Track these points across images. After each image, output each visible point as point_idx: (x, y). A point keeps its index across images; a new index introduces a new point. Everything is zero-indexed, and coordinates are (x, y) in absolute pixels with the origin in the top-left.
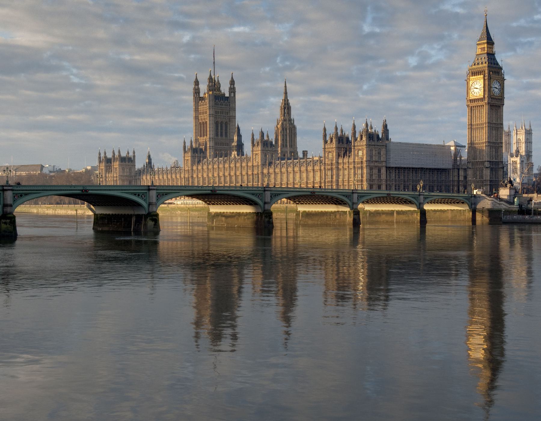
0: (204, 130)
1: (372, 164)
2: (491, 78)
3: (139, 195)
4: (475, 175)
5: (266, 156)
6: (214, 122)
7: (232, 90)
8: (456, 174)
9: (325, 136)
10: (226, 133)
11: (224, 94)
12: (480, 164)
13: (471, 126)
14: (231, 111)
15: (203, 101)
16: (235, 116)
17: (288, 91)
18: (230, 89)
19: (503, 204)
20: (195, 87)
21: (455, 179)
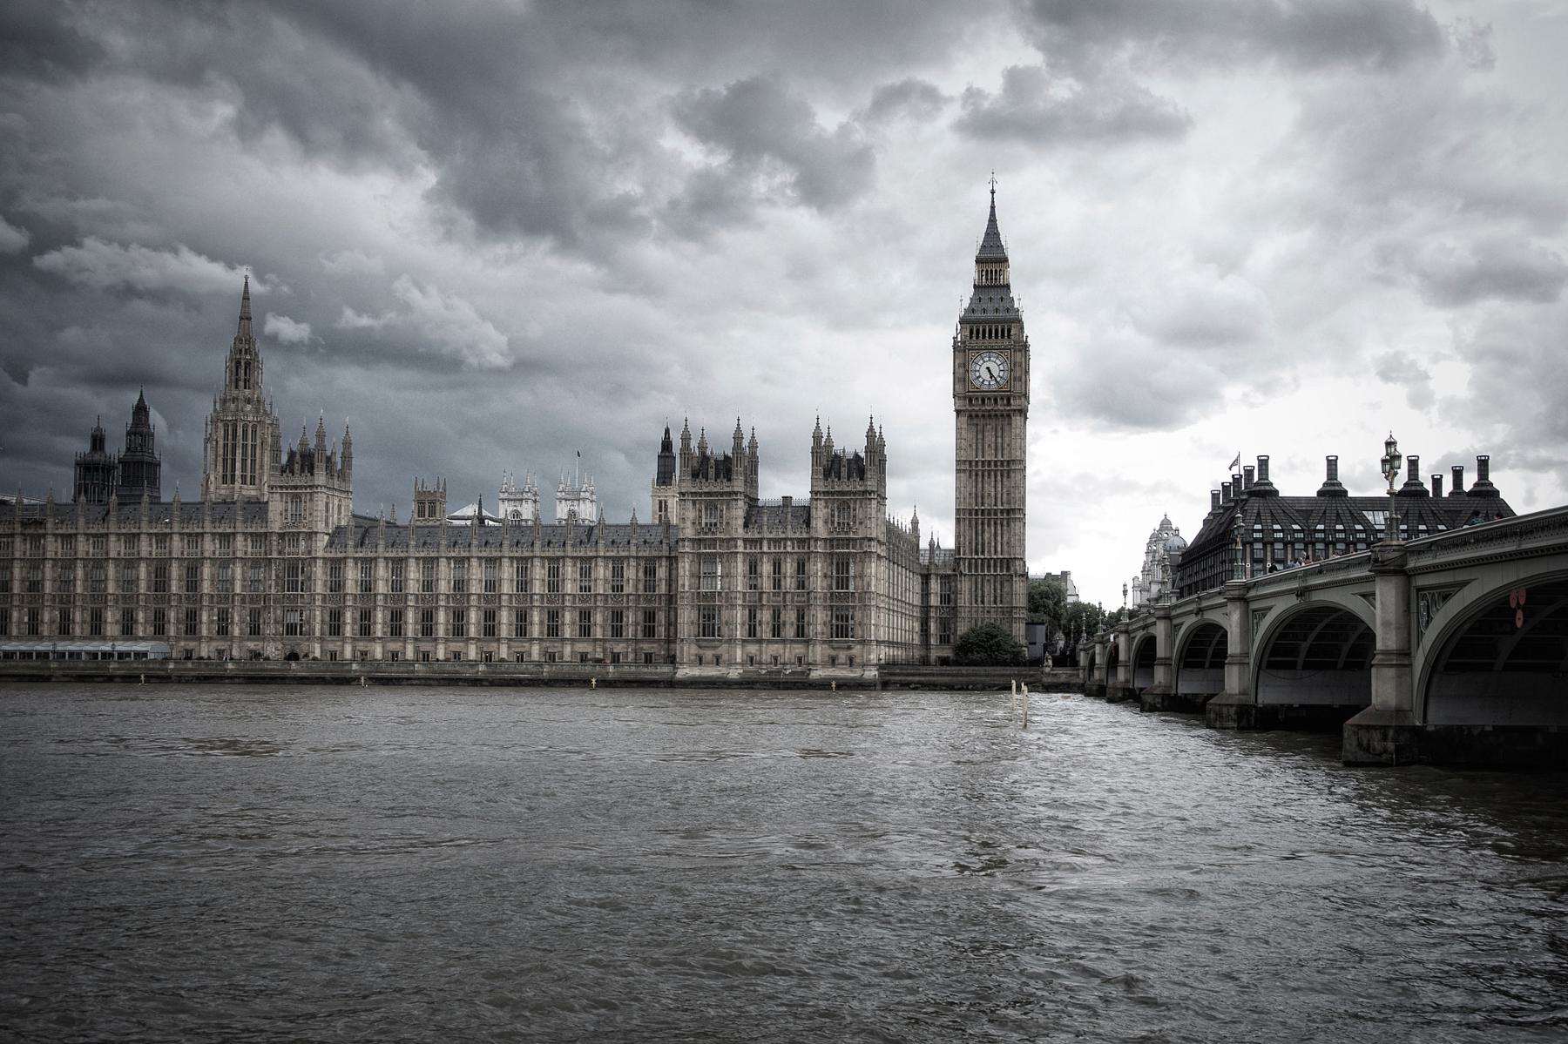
2: (1026, 351)
4: (980, 592)
8: (918, 588)
12: (995, 566)
21: (915, 603)
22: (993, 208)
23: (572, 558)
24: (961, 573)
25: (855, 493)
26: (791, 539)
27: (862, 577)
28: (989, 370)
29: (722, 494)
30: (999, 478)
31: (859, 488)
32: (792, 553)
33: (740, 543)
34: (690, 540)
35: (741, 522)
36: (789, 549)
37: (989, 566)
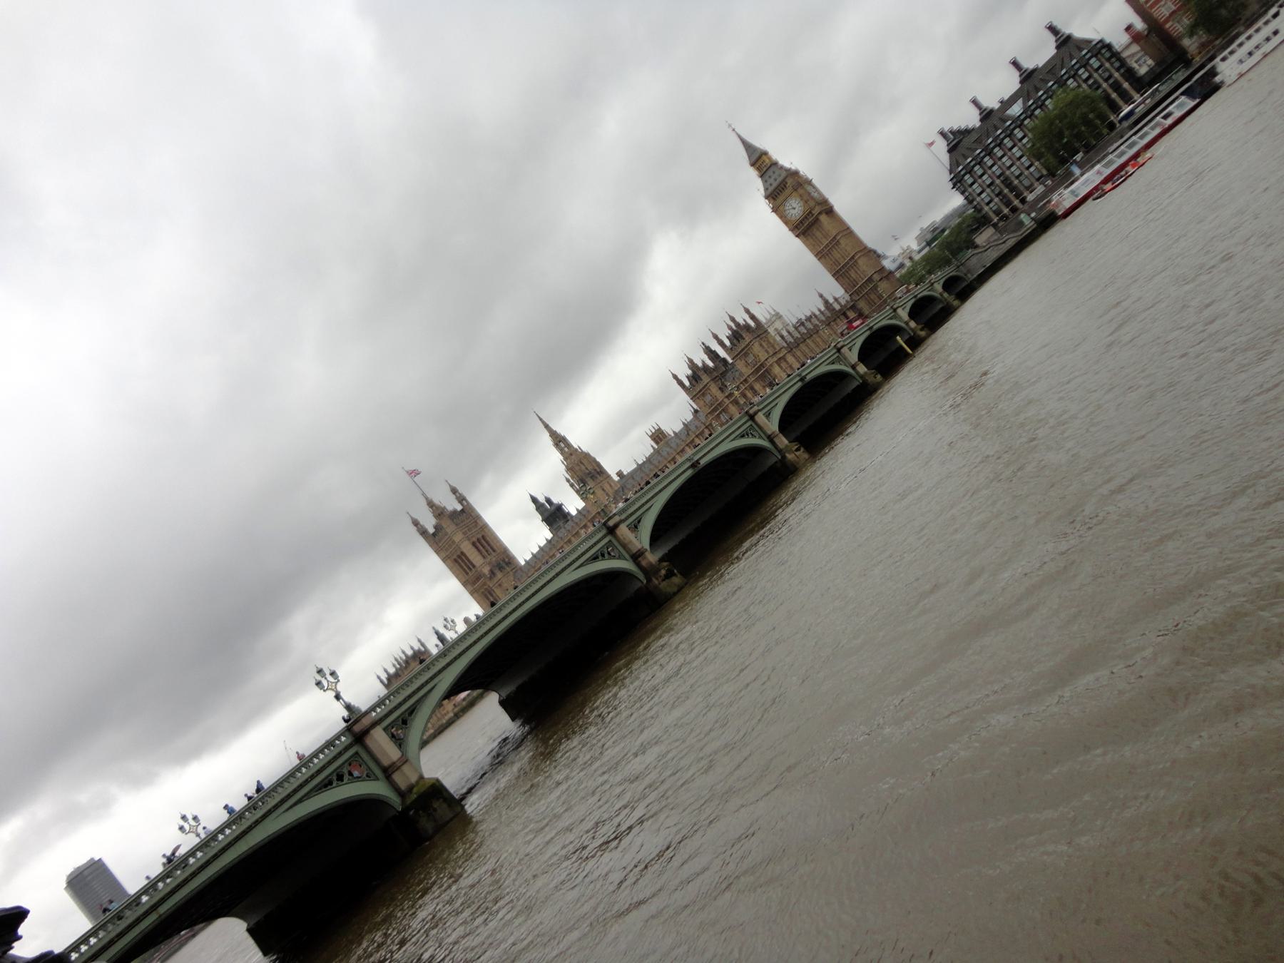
0: (466, 564)
1: (775, 359)
3: (748, 435)
5: (603, 490)
6: (471, 546)
7: (461, 499)
9: (681, 383)
10: (492, 548)
11: (455, 512)
13: (821, 255)
14: (478, 521)
15: (440, 534)
16: (486, 523)
17: (548, 423)
18: (457, 498)
19: (1008, 239)
20: (418, 528)
22: (739, 137)
23: (687, 445)
24: (856, 301)
25: (746, 347)
26: (741, 383)
27: (776, 376)
28: (795, 208)
29: (704, 388)
30: (837, 247)
31: (747, 343)
32: (745, 388)
33: (726, 400)
34: (709, 413)
35: (719, 391)
36: (744, 388)
37: (865, 287)
